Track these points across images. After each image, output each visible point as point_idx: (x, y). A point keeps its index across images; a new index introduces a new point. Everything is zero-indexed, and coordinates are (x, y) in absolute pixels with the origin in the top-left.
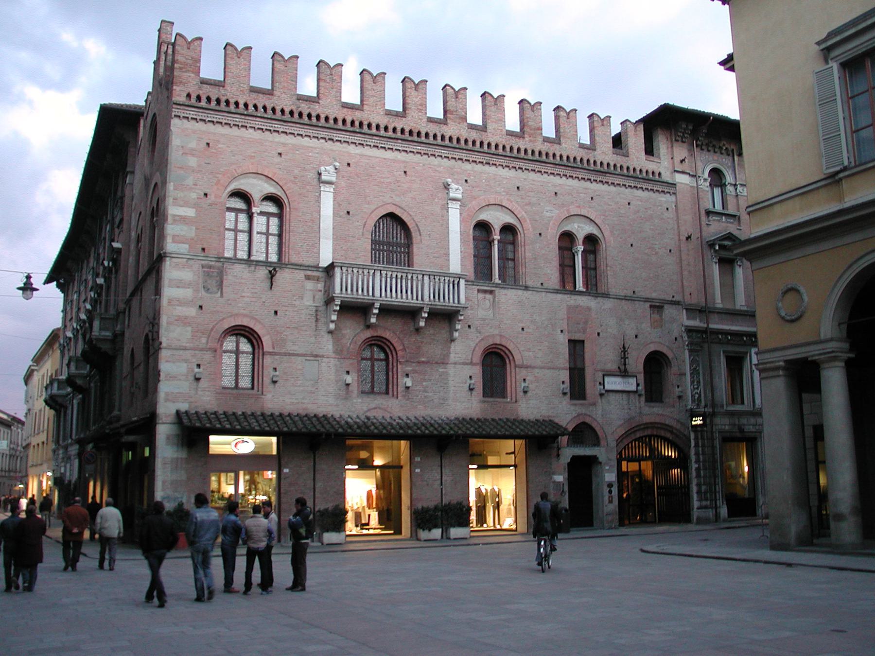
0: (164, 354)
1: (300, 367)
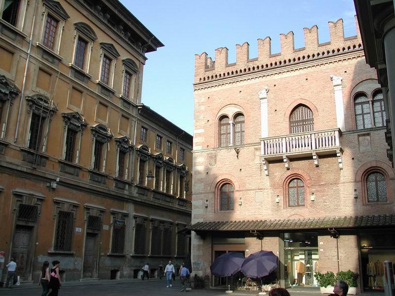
0: (193, 197)
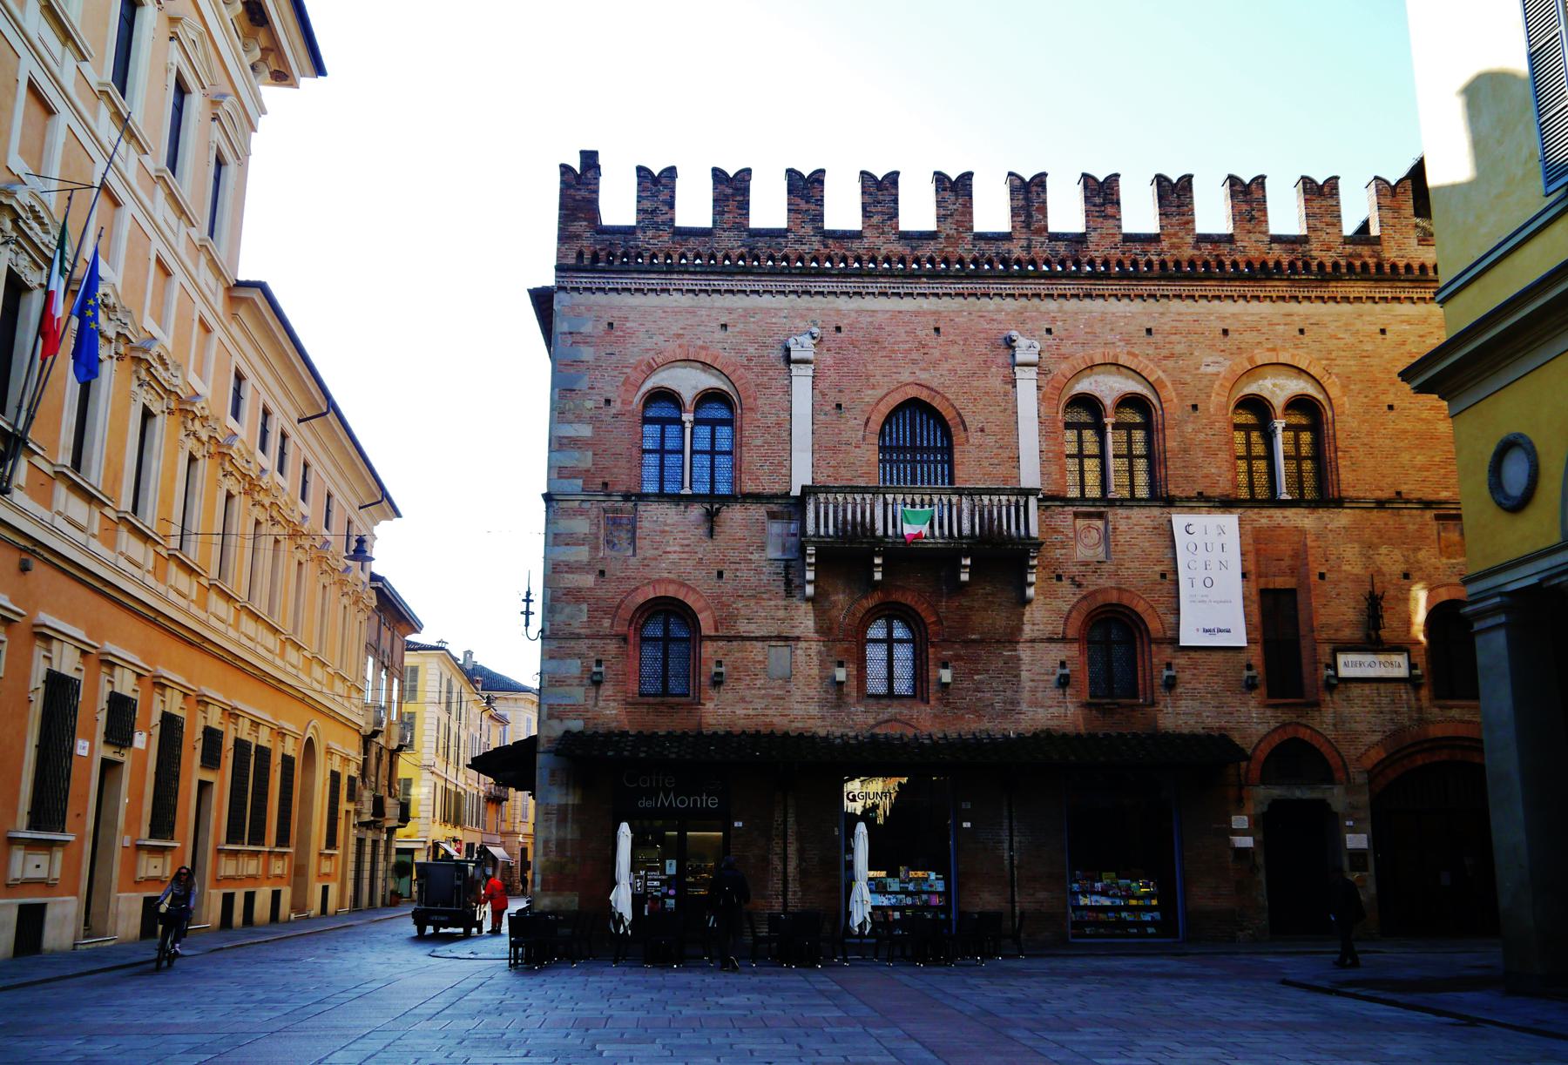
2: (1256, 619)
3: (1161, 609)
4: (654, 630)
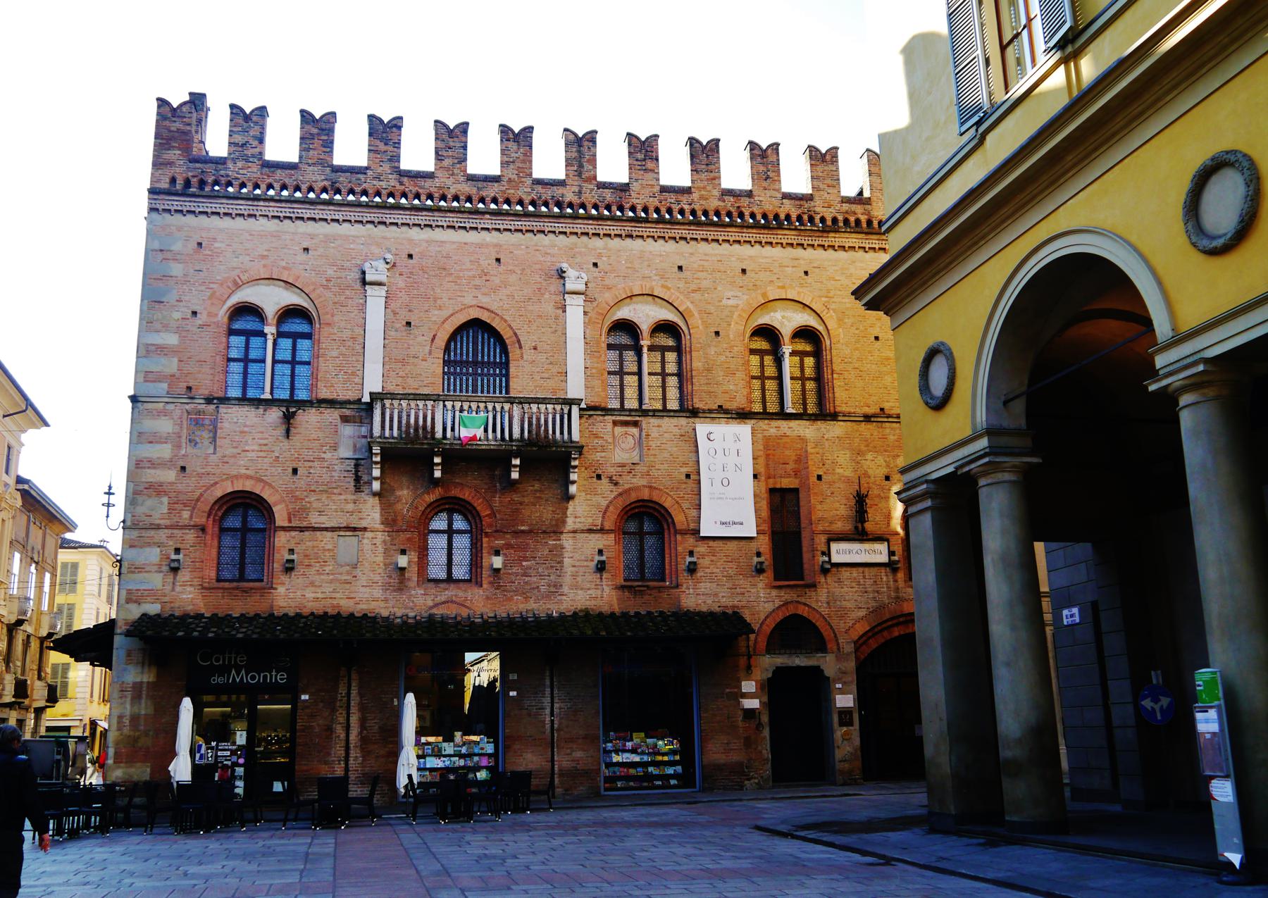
1: (330, 547)
2: (765, 513)
3: (685, 505)
4: (234, 522)
